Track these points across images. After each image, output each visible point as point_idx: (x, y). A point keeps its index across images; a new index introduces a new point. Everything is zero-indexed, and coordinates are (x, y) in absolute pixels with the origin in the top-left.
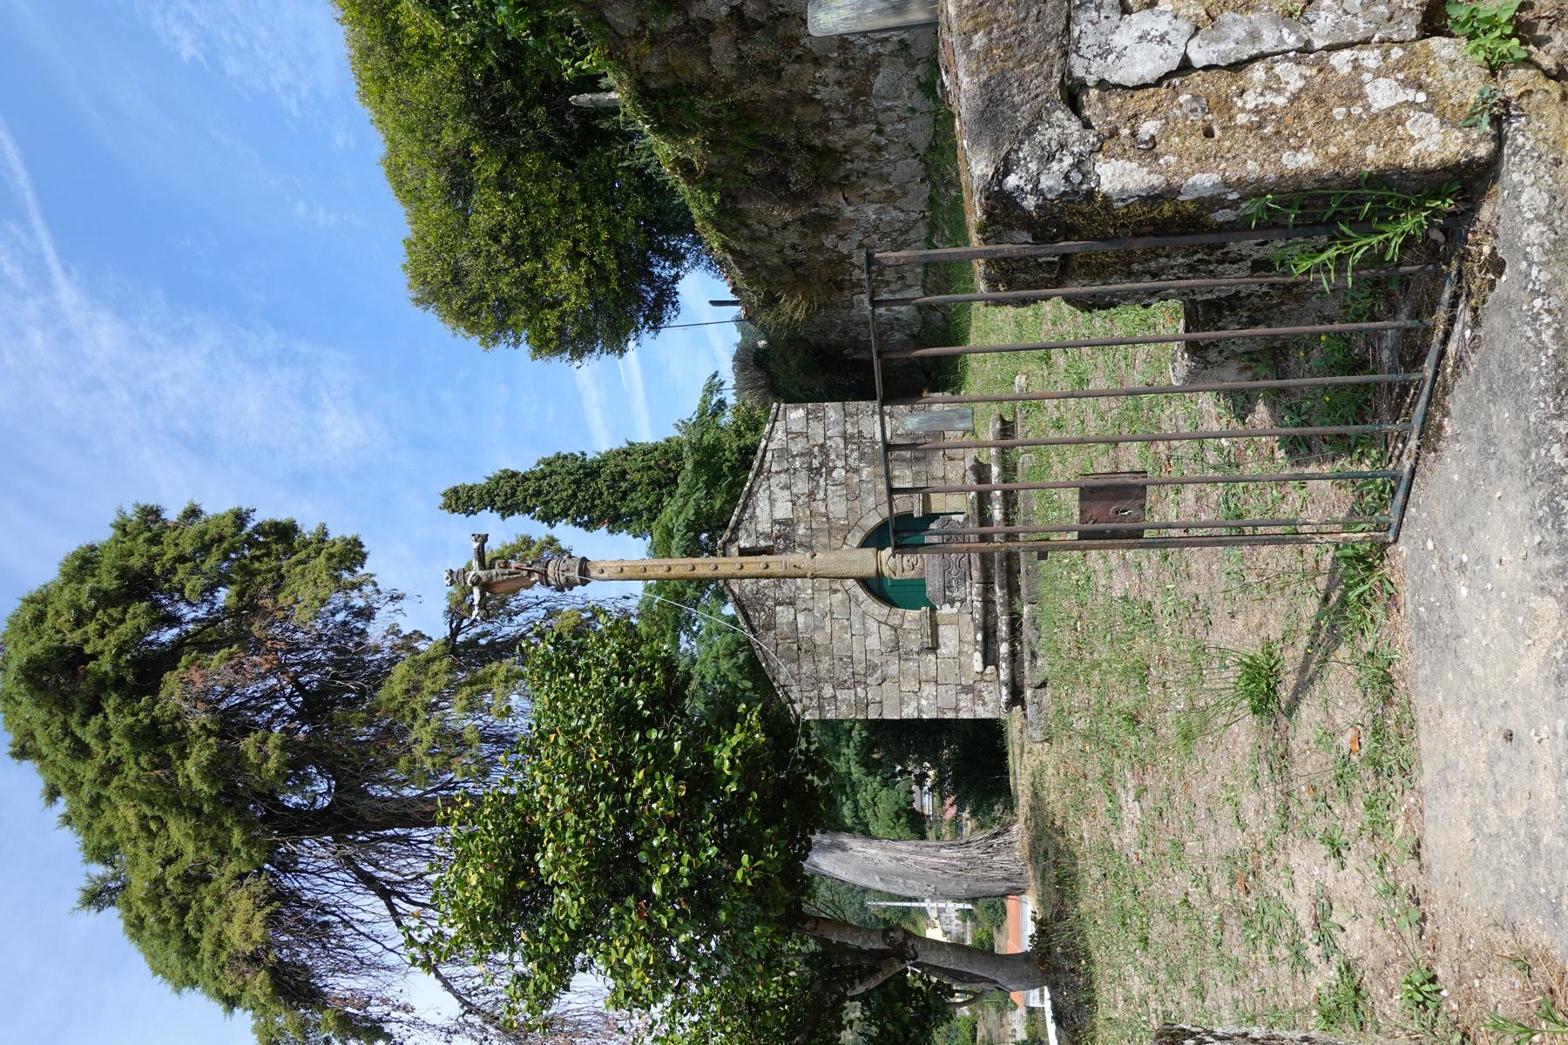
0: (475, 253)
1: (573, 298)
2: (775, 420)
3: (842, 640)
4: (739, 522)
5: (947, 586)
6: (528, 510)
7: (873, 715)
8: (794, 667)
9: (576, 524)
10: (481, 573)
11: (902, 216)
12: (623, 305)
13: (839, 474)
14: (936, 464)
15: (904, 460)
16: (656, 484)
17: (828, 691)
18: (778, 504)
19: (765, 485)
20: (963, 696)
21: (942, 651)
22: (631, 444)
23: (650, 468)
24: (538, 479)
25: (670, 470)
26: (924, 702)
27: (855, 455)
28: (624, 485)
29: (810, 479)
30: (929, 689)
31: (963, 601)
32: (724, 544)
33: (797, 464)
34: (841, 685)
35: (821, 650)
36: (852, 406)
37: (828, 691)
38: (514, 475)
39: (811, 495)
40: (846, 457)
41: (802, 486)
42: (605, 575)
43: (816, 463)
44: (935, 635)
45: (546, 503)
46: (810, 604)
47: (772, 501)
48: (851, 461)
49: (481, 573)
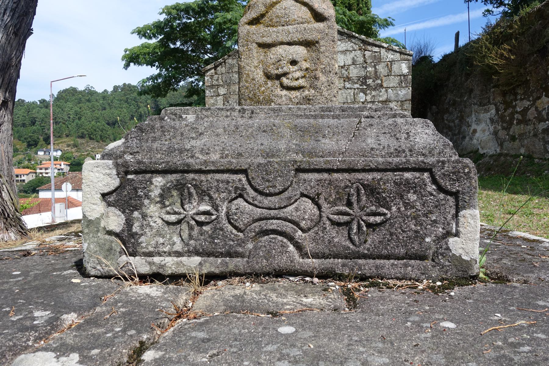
5: (186, 179)
13: (362, 97)
17: (222, 91)
19: (356, 47)
29: (359, 78)
31: (128, 240)
33: (369, 69)
37: (222, 91)
39: (348, 79)
40: (373, 102)
41: (354, 72)
43: (370, 81)
47: (344, 52)
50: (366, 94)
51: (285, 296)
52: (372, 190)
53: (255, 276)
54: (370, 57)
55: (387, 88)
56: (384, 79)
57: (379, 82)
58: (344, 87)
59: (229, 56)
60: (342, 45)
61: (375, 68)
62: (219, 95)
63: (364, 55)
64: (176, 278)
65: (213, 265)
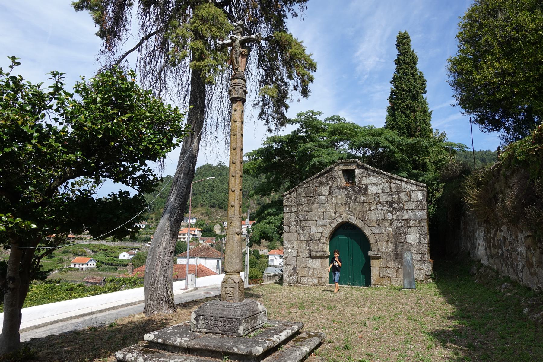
0: (507, 19)
1: (478, 77)
2: (417, 185)
3: (315, 216)
4: (367, 169)
5: (205, 317)
6: (398, 71)
7: (285, 228)
8: (304, 195)
9: (392, 92)
10: (237, 42)
11: (520, 268)
12: (482, 102)
14: (394, 264)
15: (396, 248)
16: (409, 126)
17: (294, 209)
18: (375, 187)
19: (384, 181)
20: (292, 268)
21: (310, 260)
22: (430, 113)
23: (416, 123)
24: (412, 74)
25: (416, 132)
26: (290, 250)
27: (399, 225)
28: (408, 112)
30: (295, 253)
31: (197, 325)
32: (357, 162)
34: (297, 215)
35: (311, 206)
36: (425, 224)
37: (294, 209)
38: (415, 63)
39: (379, 203)
40: (398, 220)
41: (384, 198)
42: (233, 112)
43: (395, 205)
44: (316, 257)
45: (400, 78)
46: (330, 202)
47: (376, 184)
48: (396, 222)
49: (237, 42)
50: (393, 214)
51: (216, 336)
52: (229, 321)
53: (213, 333)
54: (395, 187)
55: (408, 210)
56: (405, 203)
57: (402, 205)
58: (377, 209)
59: (299, 186)
60: (374, 179)
61: (399, 196)
62: (292, 212)
63: (390, 186)
64: (202, 332)
65: (208, 331)
